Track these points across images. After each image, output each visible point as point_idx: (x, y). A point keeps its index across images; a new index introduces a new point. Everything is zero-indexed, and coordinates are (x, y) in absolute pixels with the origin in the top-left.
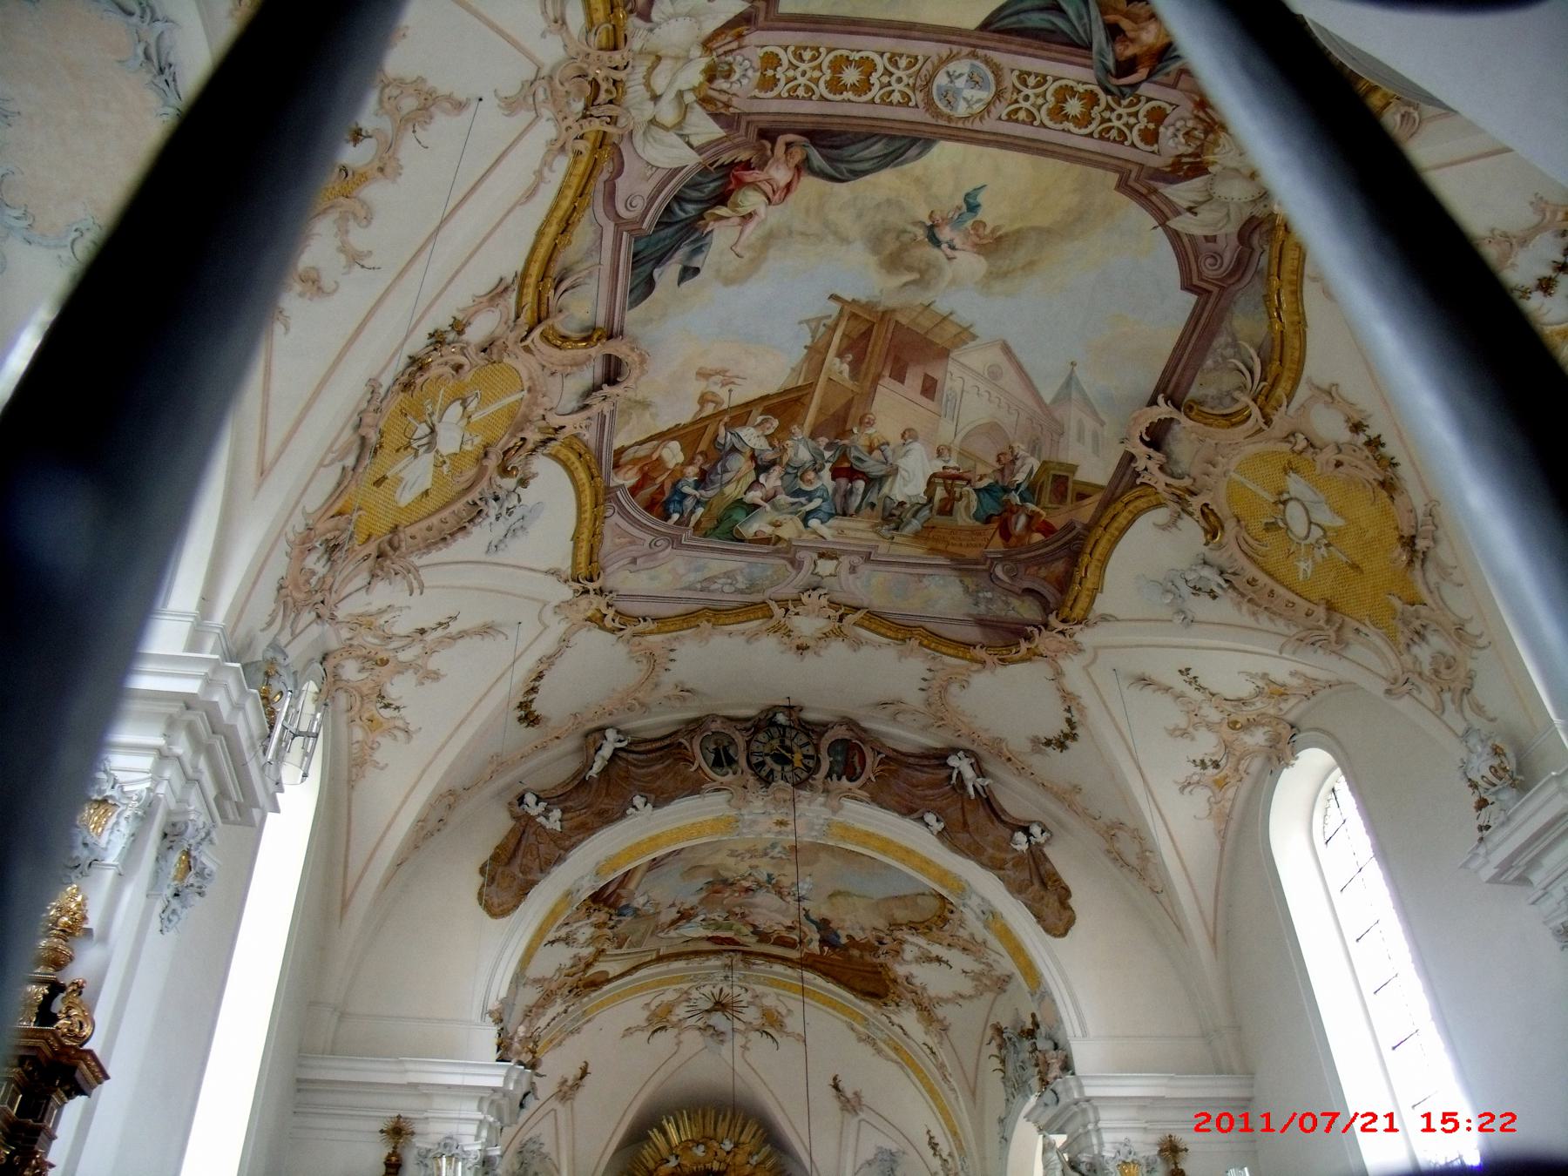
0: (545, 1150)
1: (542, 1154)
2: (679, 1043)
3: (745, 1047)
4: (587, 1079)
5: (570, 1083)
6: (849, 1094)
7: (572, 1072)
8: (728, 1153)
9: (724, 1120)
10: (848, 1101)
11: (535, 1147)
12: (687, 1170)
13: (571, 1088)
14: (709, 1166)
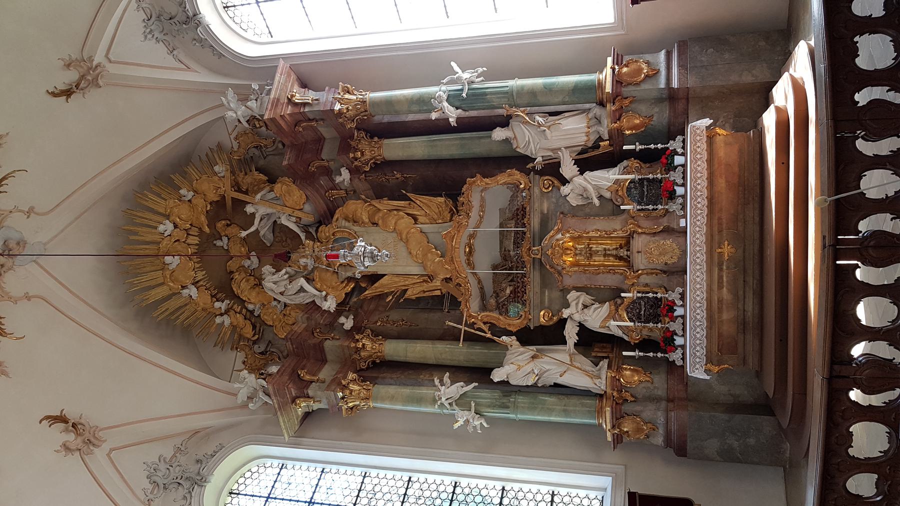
0: (169, 454)
1: (174, 456)
2: (28, 298)
3: (30, 212)
4: (72, 414)
5: (71, 437)
6: (72, 76)
7: (58, 435)
8: (176, 226)
9: (136, 234)
10: (82, 77)
11: (163, 467)
12: (200, 275)
13: (78, 434)
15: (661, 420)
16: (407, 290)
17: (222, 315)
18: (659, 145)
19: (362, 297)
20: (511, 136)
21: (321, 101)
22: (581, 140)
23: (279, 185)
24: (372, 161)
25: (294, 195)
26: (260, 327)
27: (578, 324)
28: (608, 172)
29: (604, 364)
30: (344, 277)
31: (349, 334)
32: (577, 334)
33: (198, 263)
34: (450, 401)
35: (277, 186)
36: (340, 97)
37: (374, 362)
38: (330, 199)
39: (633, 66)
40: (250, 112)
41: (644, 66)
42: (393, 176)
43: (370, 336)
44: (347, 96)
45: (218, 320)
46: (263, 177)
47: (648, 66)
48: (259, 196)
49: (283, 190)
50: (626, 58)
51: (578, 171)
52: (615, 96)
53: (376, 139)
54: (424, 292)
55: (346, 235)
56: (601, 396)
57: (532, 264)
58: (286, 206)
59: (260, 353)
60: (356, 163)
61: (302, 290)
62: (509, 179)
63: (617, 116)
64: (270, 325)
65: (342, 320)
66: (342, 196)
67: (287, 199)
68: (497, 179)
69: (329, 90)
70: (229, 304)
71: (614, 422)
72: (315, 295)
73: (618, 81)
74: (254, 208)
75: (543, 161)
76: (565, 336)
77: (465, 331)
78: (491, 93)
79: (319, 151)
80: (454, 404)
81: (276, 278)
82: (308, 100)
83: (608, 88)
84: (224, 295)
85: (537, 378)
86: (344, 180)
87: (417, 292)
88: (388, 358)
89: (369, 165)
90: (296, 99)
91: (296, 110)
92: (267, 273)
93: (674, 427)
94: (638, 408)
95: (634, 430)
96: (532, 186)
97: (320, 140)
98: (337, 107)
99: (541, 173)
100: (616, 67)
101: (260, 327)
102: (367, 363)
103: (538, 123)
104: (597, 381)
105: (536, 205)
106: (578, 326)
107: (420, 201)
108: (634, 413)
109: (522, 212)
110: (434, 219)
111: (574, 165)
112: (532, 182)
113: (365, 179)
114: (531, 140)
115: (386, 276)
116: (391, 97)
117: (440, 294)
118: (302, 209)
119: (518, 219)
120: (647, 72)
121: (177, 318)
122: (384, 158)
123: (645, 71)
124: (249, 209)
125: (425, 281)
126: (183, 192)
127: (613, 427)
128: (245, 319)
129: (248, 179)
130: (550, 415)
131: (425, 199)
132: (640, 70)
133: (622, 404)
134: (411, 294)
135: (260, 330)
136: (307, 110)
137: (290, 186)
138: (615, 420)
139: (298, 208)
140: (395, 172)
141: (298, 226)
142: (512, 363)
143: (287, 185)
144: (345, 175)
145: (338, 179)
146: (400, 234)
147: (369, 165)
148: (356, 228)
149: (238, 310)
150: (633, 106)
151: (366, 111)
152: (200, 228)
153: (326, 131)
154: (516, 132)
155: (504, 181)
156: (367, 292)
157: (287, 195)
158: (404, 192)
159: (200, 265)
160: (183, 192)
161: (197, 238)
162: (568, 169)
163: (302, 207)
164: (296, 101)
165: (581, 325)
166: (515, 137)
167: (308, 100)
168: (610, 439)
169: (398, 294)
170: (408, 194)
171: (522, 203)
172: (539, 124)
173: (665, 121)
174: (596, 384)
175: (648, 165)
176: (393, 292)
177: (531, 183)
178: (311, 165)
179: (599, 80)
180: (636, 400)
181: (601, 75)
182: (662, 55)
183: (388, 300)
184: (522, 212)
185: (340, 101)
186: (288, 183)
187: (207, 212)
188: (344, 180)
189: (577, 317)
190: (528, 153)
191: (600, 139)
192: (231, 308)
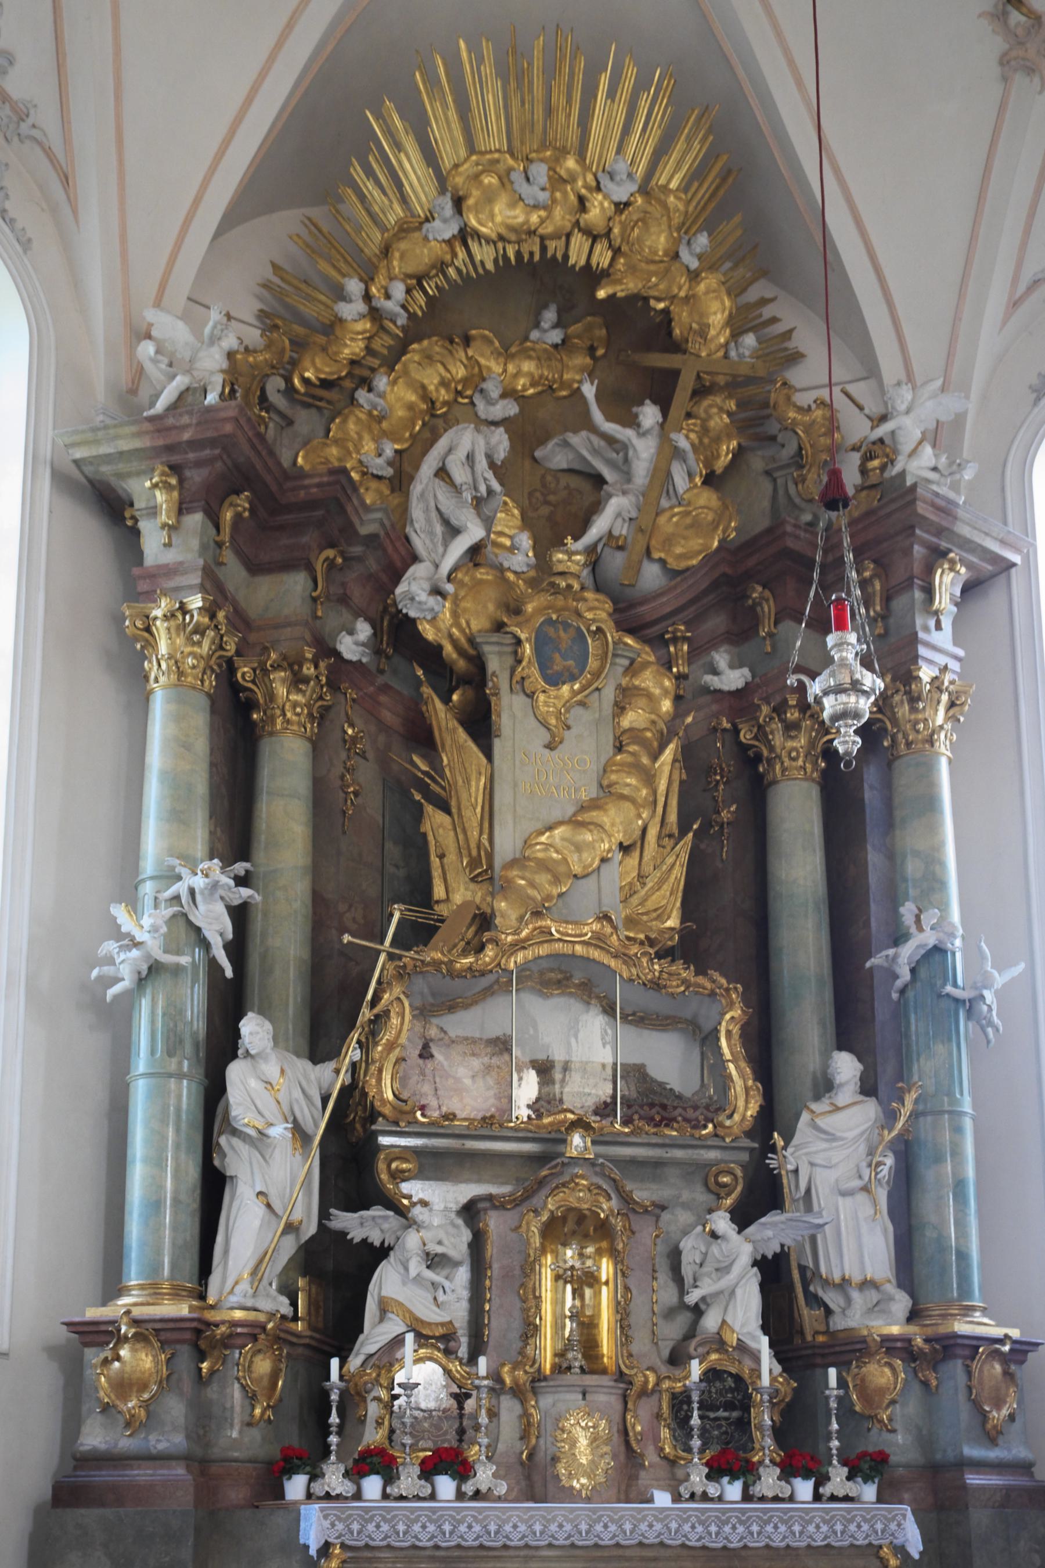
12: (485, 255)
14: (554, 247)
15: (159, 1442)
16: (448, 812)
17: (367, 297)
19: (426, 690)
24: (765, 753)
26: (329, 402)
27: (386, 1245)
29: (283, 1306)
30: (486, 649)
31: (327, 650)
32: (364, 1241)
33: (519, 254)
34: (185, 898)
35: (708, 498)
37: (251, 705)
38: (668, 632)
40: (906, 447)
43: (320, 703)
45: (354, 286)
54: (441, 857)
55: (593, 664)
56: (202, 1297)
57: (537, 1135)
59: (263, 390)
61: (453, 531)
62: (738, 1089)
64: (328, 431)
65: (364, 630)
67: (675, 519)
70: (395, 323)
71: (150, 1326)
72: (437, 566)
74: (652, 428)
76: (368, 1209)
77: (378, 953)
78: (951, 1054)
80: (177, 909)
81: (482, 464)
82: (940, 603)
84: (420, 313)
85: (252, 1132)
87: (440, 839)
88: (266, 747)
92: (494, 440)
93: (141, 1474)
94: (187, 1384)
95: (126, 1376)
96: (723, 1144)
101: (329, 402)
102: (250, 685)
104: (244, 1286)
105: (678, 1154)
106: (383, 1243)
107: (673, 865)
108: (175, 1377)
109: (658, 1118)
110: (631, 896)
115: (484, 761)
116: (942, 813)
117: (436, 897)
119: (641, 1106)
121: (370, 173)
122: (775, 782)
124: (649, 414)
125: (474, 863)
126: (702, 240)
127: (136, 1322)
128: (353, 363)
130: (146, 1160)
131: (679, 873)
133: (196, 1346)
134: (435, 821)
135: (321, 399)
136: (918, 595)
138: (158, 1326)
141: (600, 539)
142: (282, 1071)
146: (594, 805)
148: (609, 694)
149: (377, 345)
151: (908, 744)
152: (608, 275)
156: (439, 705)
158: (695, 827)
159: (512, 258)
160: (702, 240)
161: (582, 262)
163: (656, 555)
164: (939, 571)
165: (382, 1252)
167: (940, 603)
168: (93, 1313)
169: (433, 786)
170: (691, 835)
171: (680, 1119)
174: (236, 1283)
176: (443, 776)
177: (733, 1141)
180: (201, 1381)
183: (416, 759)
184: (658, 1118)
187: (646, 299)
189: (412, 1240)
192: (383, 328)
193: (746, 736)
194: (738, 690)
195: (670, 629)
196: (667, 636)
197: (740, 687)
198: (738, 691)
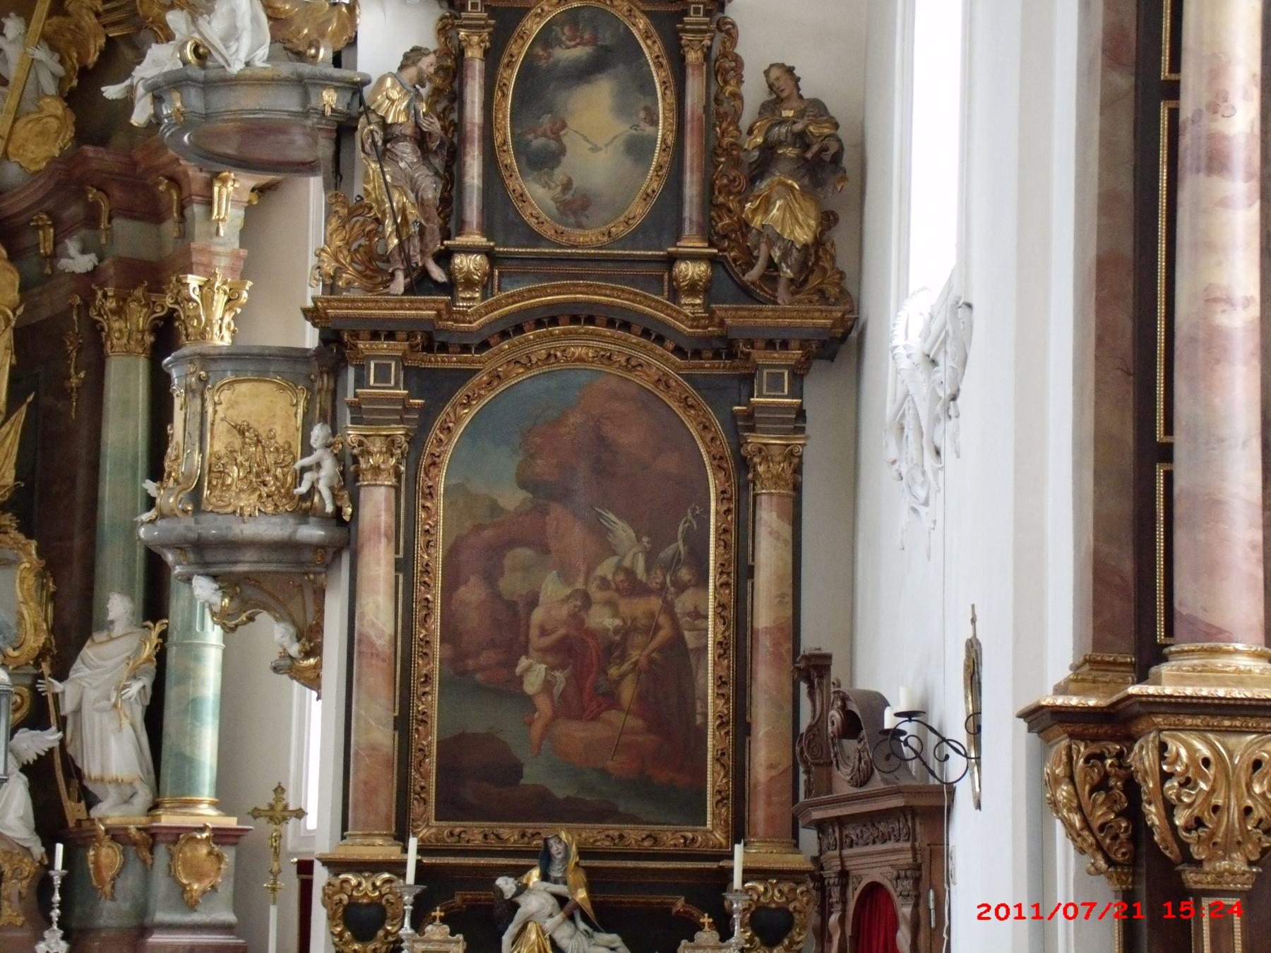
18: (58, 911)
20: (115, 631)
21: (216, 240)
22: (92, 767)
23: (60, 112)
25: (37, 145)
28: (21, 818)
35: (56, 107)
36: (217, 284)
38: (32, 220)
39: (209, 865)
41: (206, 884)
42: (76, 368)
44: (220, 300)
46: (93, 58)
47: (204, 892)
48: (42, 54)
49: (49, 119)
50: (229, 854)
51: (28, 762)
52: (152, 837)
53: (149, 339)
58: (15, 120)
60: (100, 294)
62: (28, 626)
63: (117, 835)
66: (41, 246)
67: (30, 125)
68: (32, 600)
69: (238, 257)
73: (178, 836)
75: (56, 696)
79: (130, 213)
82: (219, 214)
83: (167, 819)
86: (72, 258)
89: (100, 319)
90: (220, 188)
91: (196, 187)
97: (154, 215)
98: (193, 281)
99: (33, 688)
100: (204, 835)
103: (125, 687)
107: (8, 433)
111: (38, 755)
112: (19, 671)
113: (71, 306)
114: (98, 671)
118: (8, 158)
120: (191, 890)
123: (196, 887)
129: (89, 21)
132: (200, 877)
137: (56, 139)
139: (10, 149)
140: (82, 375)
143: (58, 133)
144: (79, 262)
145: (72, 246)
147: (100, 319)
150: (138, 864)
151: (187, 336)
153: (170, 228)
154: (122, 640)
155: (26, 616)
157: (38, 128)
162: (35, 743)
163: (13, 159)
166: (111, 639)
167: (219, 214)
170: (24, 408)
172: (123, 689)
173: (102, 922)
175: (24, 892)
177: (14, 669)
178: (101, 194)
179: (201, 802)
181: (206, 806)
182: (229, 917)
185: (206, 288)
186: (61, 137)
188: (72, 258)
190: (78, 664)
191: (90, 800)
193: (93, 314)
194: (88, 272)
195: (35, 218)
196: (32, 224)
197: (89, 269)
198: (88, 274)
